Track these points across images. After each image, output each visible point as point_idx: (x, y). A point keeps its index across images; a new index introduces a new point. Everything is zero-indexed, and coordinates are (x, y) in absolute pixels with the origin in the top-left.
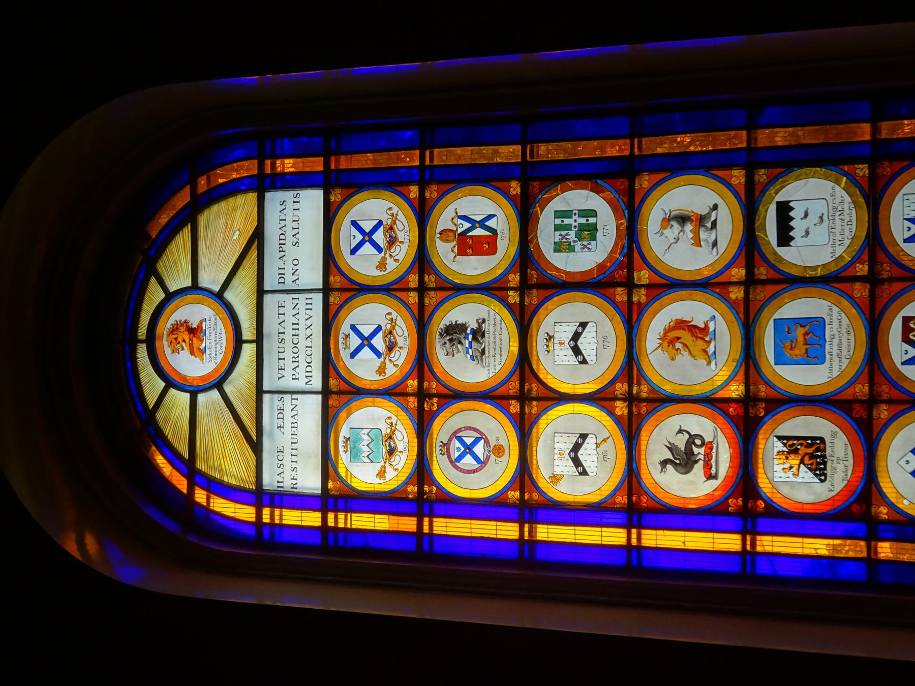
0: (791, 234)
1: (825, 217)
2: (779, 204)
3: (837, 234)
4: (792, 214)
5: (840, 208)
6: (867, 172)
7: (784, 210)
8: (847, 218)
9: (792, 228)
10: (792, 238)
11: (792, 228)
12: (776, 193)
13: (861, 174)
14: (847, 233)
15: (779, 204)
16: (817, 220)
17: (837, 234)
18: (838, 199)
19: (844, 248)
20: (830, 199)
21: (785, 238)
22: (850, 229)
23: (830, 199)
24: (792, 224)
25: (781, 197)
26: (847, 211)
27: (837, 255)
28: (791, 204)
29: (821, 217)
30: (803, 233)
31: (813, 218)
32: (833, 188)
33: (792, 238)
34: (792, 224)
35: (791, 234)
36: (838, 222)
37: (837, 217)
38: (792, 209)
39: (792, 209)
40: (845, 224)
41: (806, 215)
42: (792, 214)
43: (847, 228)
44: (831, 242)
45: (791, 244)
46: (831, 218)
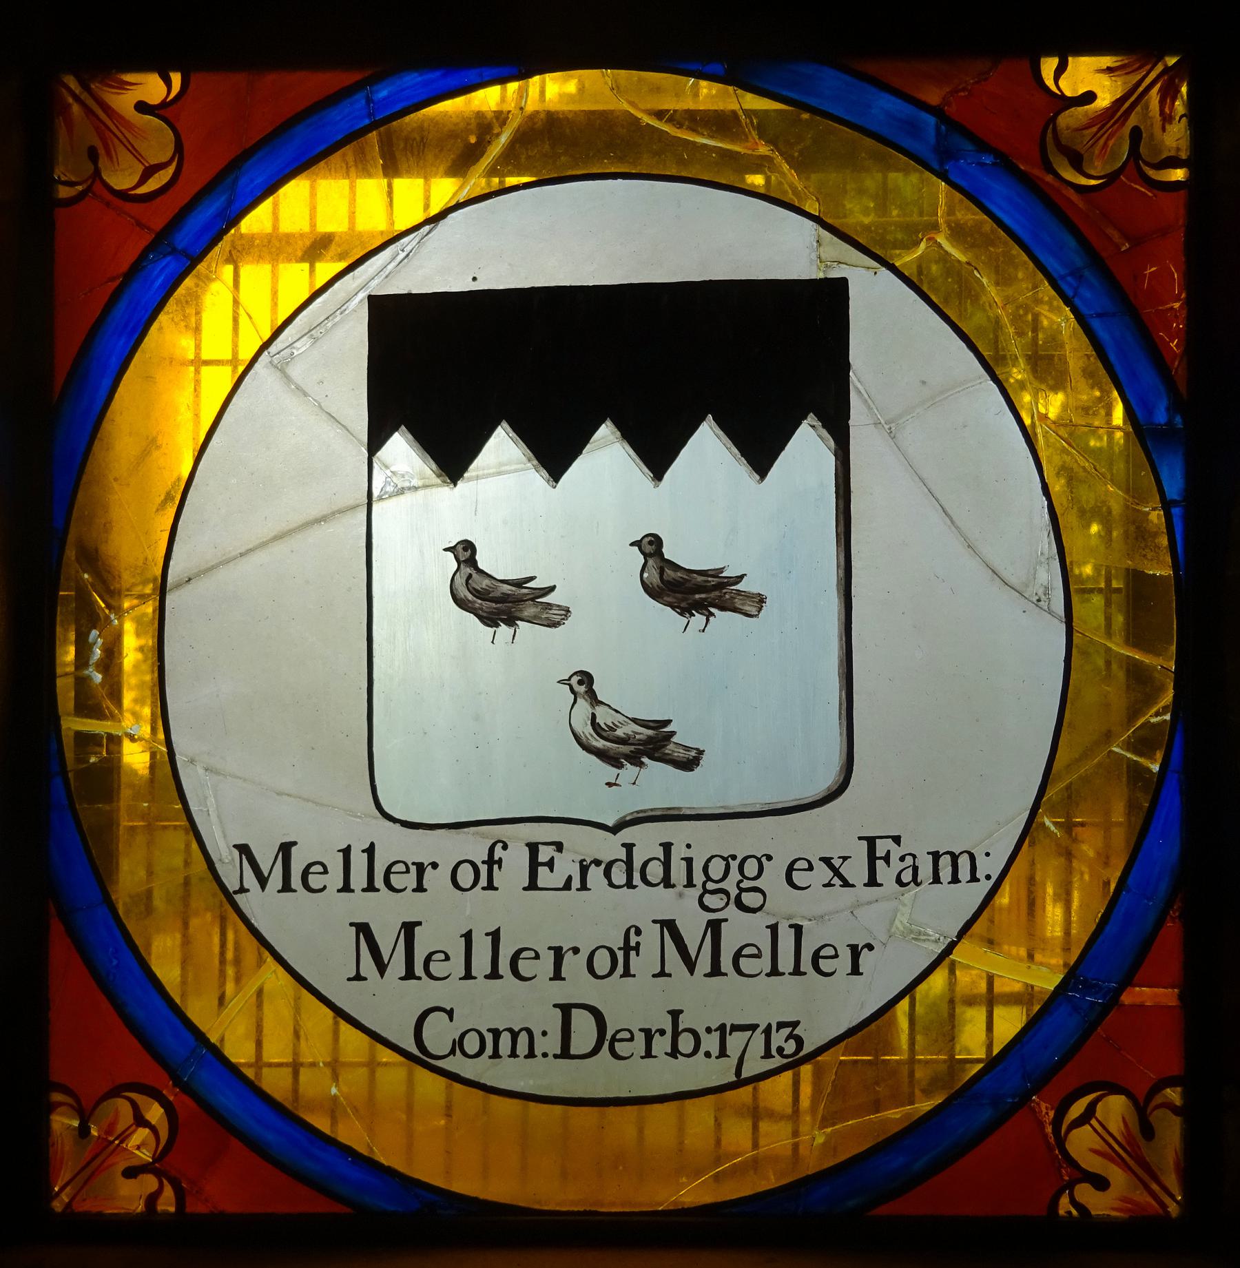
0: (502, 448)
1: (656, 784)
2: (815, 313)
3: (479, 911)
4: (708, 447)
5: (741, 929)
6: (1100, 1204)
7: (746, 365)
8: (633, 1002)
9: (555, 455)
10: (452, 460)
11: (555, 455)
12: (942, 294)
13: (1082, 1143)
14: (488, 1004)
15: (815, 313)
16: (630, 698)
17: (479, 911)
18: (830, 915)
19: (328, 957)
20: (835, 830)
21: (450, 374)
22: (521, 1040)
23: (835, 830)
24: (607, 456)
25: (888, 330)
26: (706, 1000)
27: (261, 905)
28: (808, 446)
29: (654, 744)
30: (498, 562)
31: (647, 659)
32: (950, 865)
33: (452, 460)
34: (607, 456)
35: (502, 448)
36: (602, 914)
37: (647, 904)
38: (760, 451)
39: (760, 451)
40: (578, 986)
41: (690, 592)
42: (708, 447)
43: (529, 1004)
44: (396, 846)
45: (400, 450)
46: (647, 840)
